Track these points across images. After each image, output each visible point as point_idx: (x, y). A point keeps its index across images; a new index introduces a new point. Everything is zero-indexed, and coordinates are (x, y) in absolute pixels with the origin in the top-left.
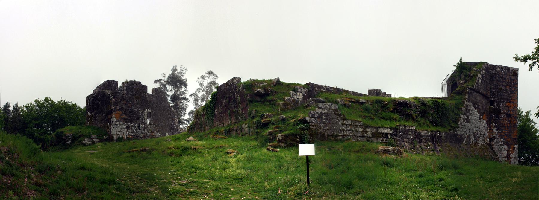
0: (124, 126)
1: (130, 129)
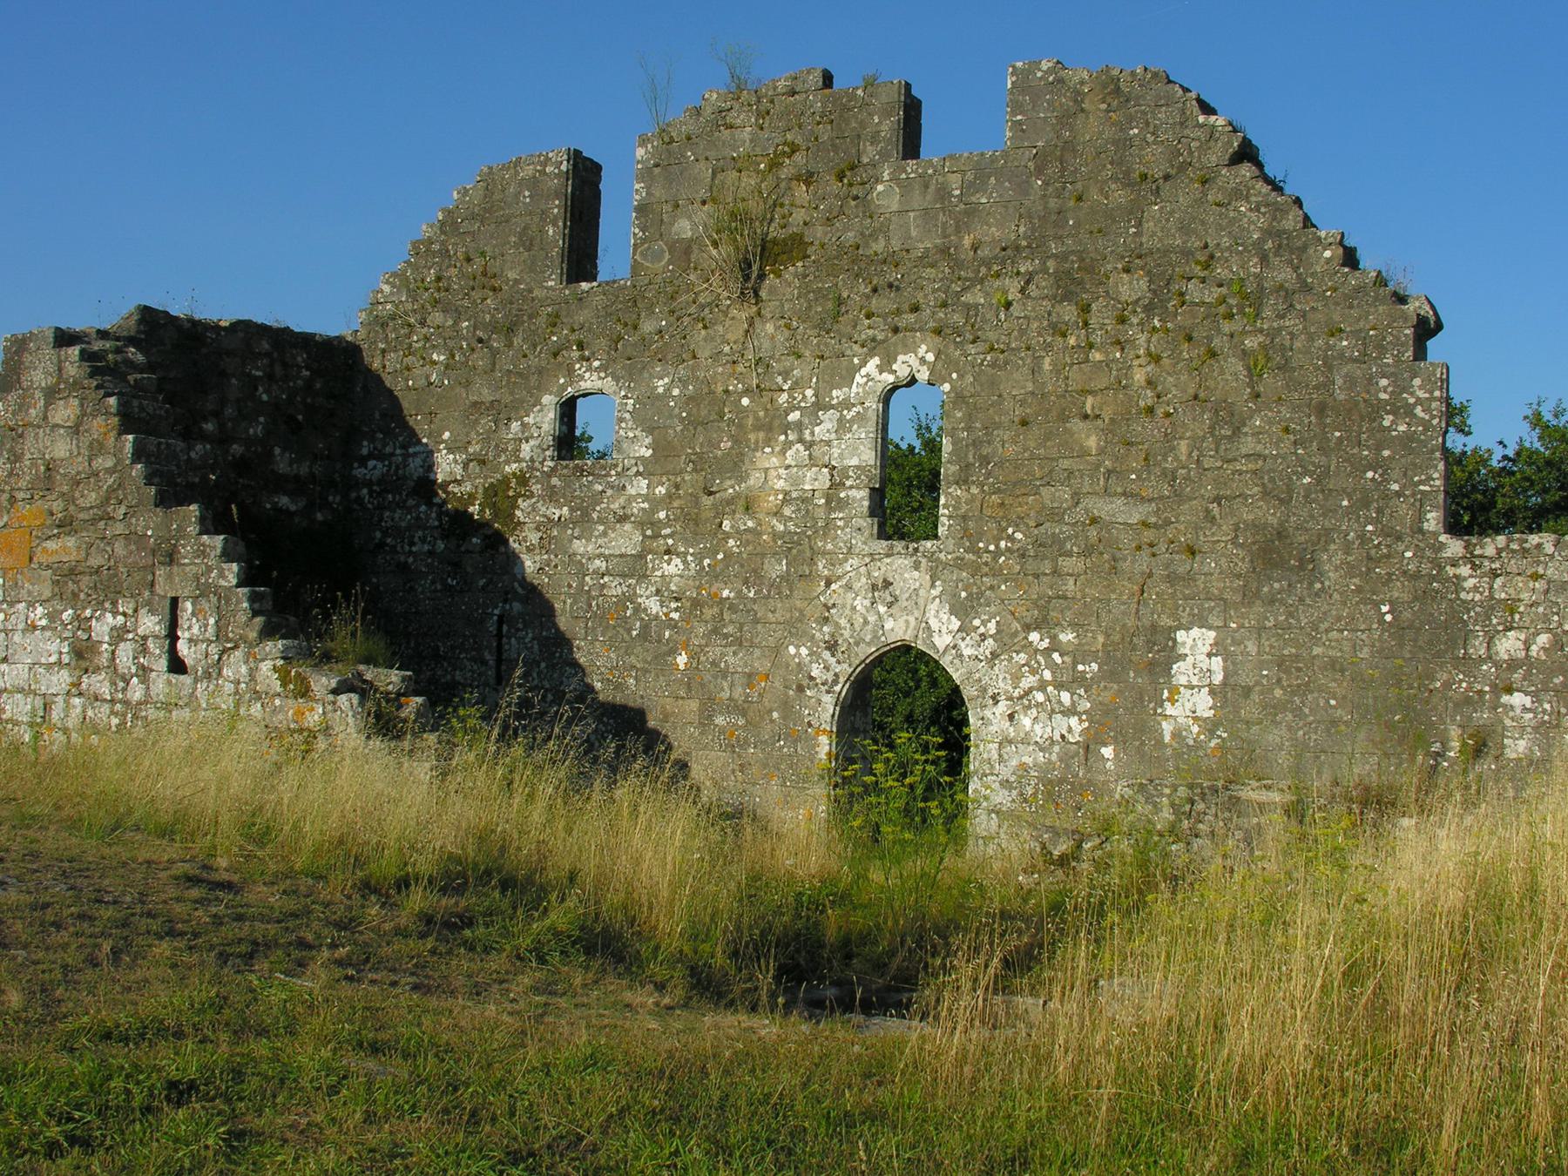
0: (54, 646)
1: (97, 670)
